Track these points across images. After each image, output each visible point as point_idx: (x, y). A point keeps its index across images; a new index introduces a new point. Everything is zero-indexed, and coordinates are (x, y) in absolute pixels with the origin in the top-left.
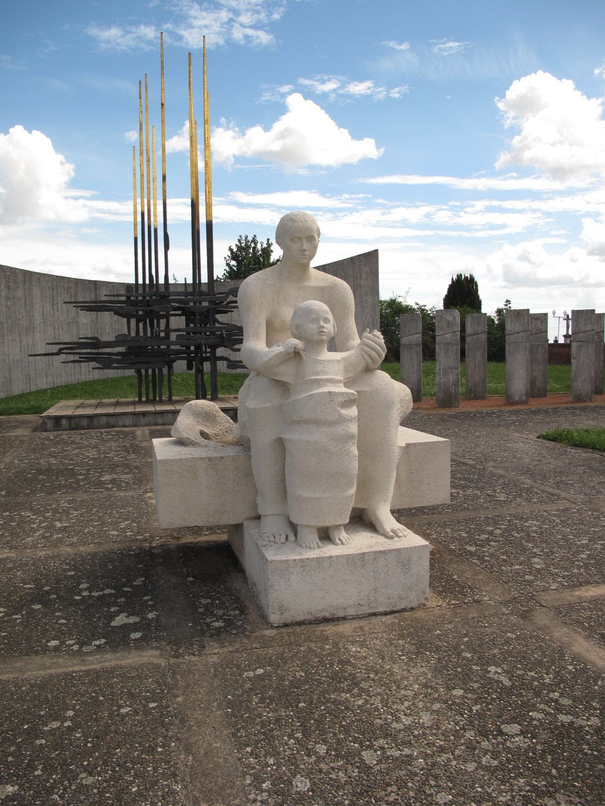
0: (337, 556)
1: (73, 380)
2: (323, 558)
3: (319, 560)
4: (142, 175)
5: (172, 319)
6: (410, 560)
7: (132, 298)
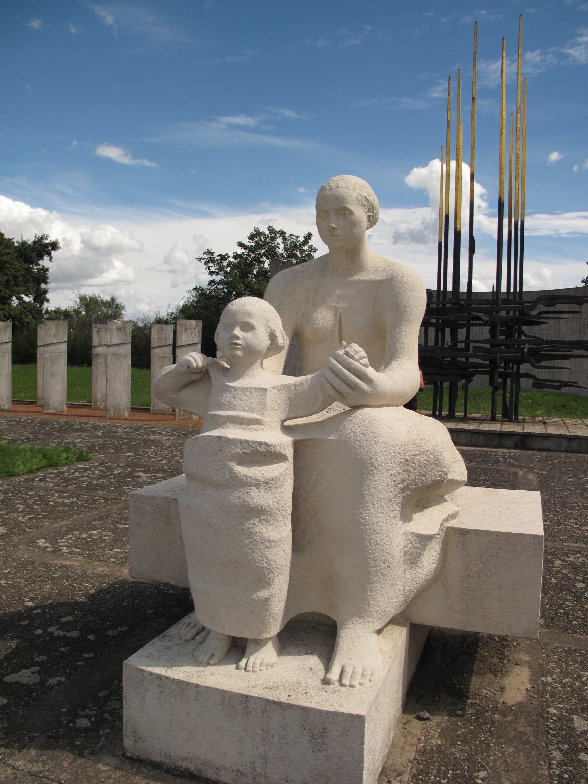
0: (207, 688)
2: (188, 683)
3: (182, 685)
4: (448, 176)
5: (474, 330)
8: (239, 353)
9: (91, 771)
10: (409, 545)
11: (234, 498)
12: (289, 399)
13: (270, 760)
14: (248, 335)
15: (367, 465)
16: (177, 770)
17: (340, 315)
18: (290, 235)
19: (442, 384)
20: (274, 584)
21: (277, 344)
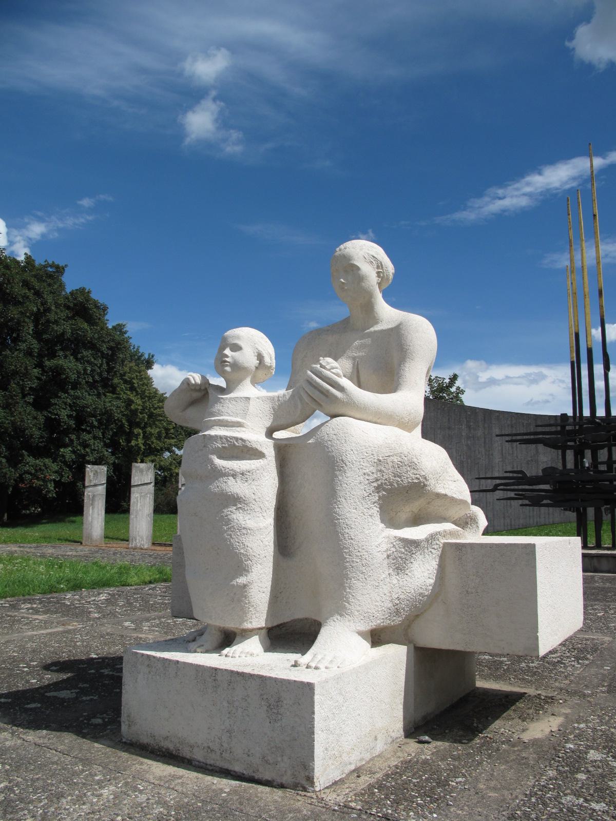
0: (184, 663)
1: (594, 534)
6: (279, 700)
7: (568, 428)
8: (228, 369)
9: (85, 747)
10: (392, 549)
11: (214, 487)
12: (274, 409)
13: (234, 734)
14: (236, 354)
15: (338, 462)
16: (159, 751)
17: (358, 362)
18: (436, 377)
19: (585, 510)
20: (252, 572)
21: (264, 363)
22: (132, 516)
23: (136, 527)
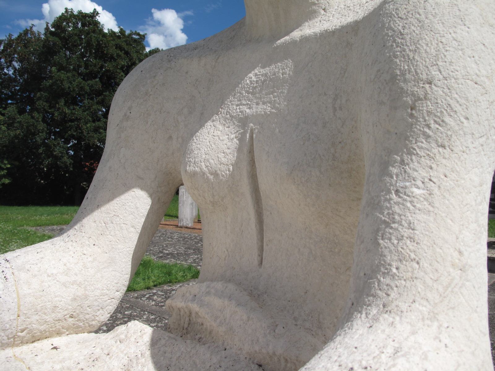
17: (251, 137)
22: (180, 205)
23: (183, 212)
